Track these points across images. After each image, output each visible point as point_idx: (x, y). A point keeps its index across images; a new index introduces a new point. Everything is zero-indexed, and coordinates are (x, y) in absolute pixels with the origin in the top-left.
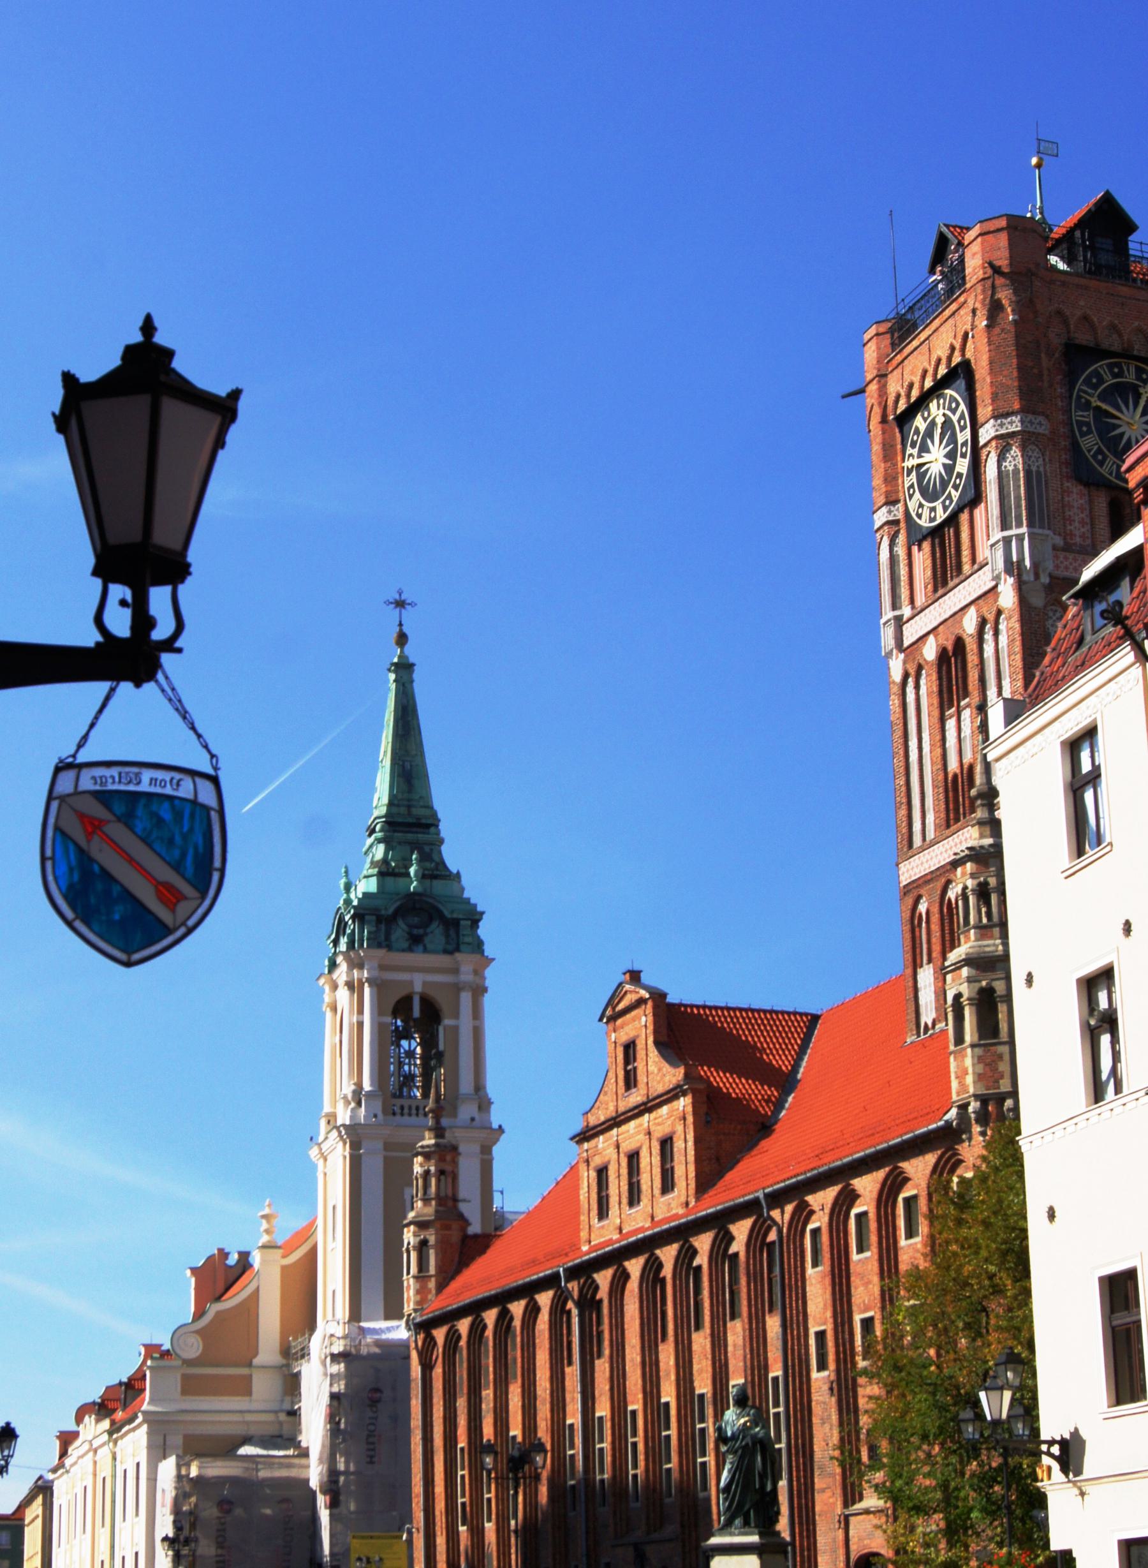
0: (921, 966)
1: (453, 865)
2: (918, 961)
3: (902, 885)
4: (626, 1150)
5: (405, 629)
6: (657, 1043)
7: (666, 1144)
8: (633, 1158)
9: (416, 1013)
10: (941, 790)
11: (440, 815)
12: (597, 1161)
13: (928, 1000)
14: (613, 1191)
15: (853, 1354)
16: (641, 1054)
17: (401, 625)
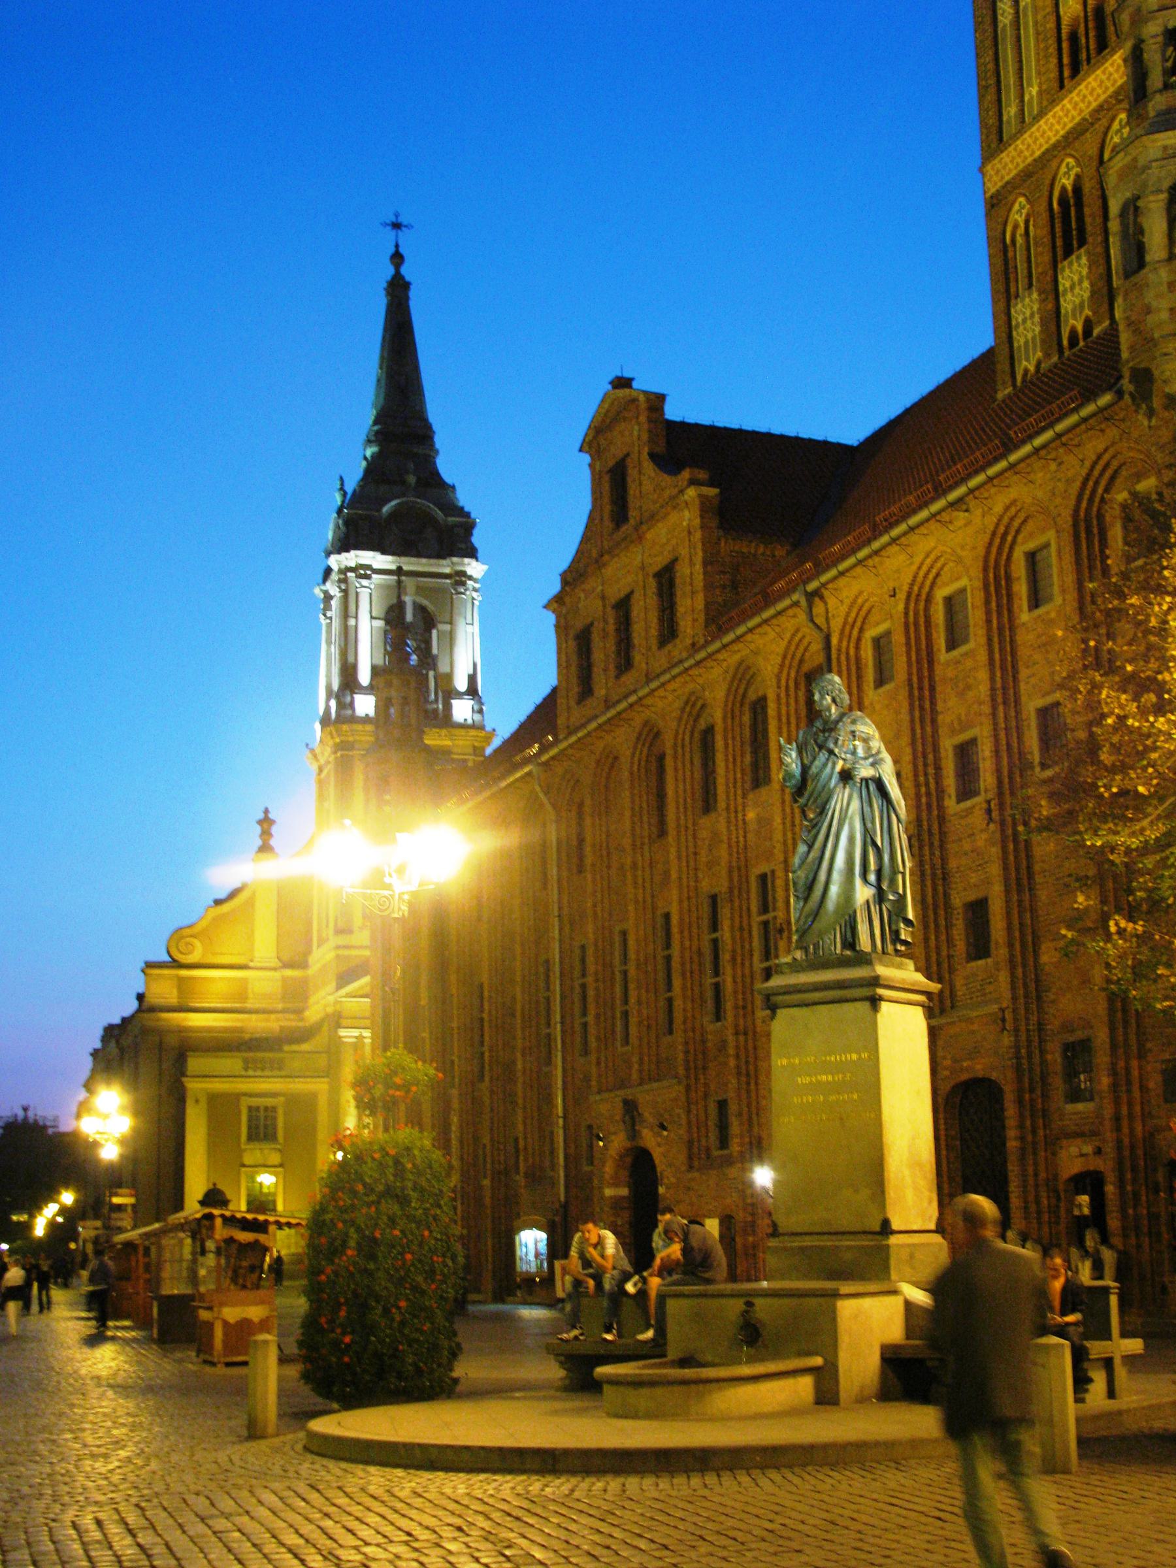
0: (1017, 296)
1: (447, 474)
2: (1013, 290)
3: (988, 195)
4: (613, 601)
5: (401, 250)
6: (653, 456)
7: (666, 579)
8: (623, 606)
9: (409, 617)
10: (1052, 42)
11: (435, 428)
12: (579, 624)
13: (1030, 336)
14: (598, 656)
15: (941, 792)
16: (632, 473)
17: (397, 246)
